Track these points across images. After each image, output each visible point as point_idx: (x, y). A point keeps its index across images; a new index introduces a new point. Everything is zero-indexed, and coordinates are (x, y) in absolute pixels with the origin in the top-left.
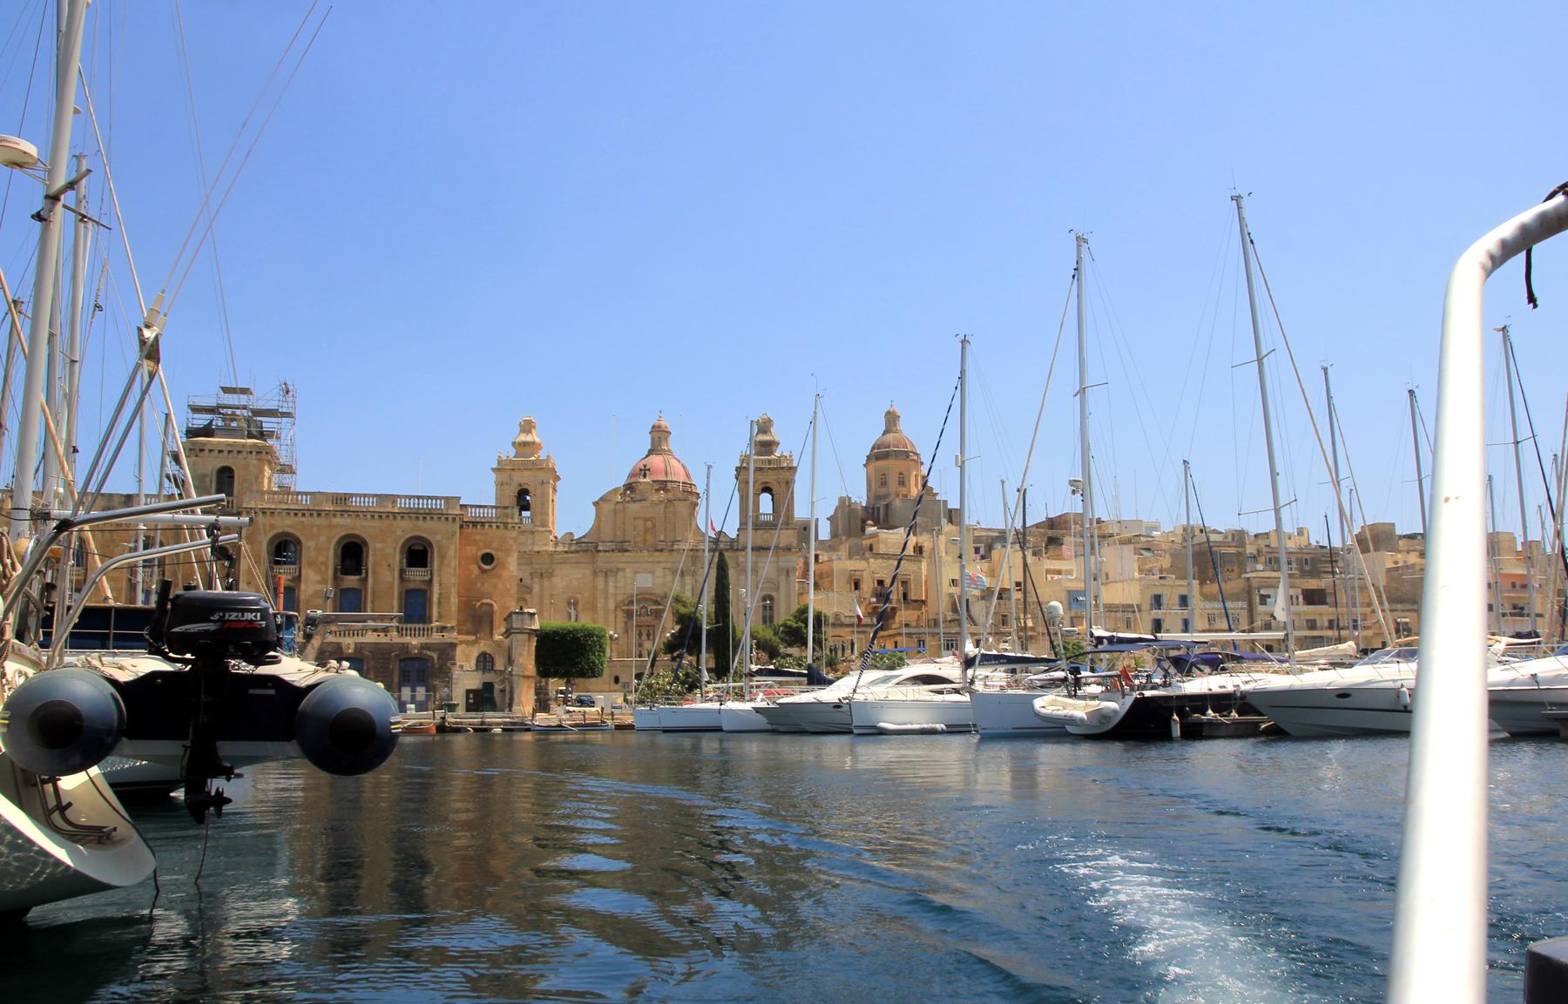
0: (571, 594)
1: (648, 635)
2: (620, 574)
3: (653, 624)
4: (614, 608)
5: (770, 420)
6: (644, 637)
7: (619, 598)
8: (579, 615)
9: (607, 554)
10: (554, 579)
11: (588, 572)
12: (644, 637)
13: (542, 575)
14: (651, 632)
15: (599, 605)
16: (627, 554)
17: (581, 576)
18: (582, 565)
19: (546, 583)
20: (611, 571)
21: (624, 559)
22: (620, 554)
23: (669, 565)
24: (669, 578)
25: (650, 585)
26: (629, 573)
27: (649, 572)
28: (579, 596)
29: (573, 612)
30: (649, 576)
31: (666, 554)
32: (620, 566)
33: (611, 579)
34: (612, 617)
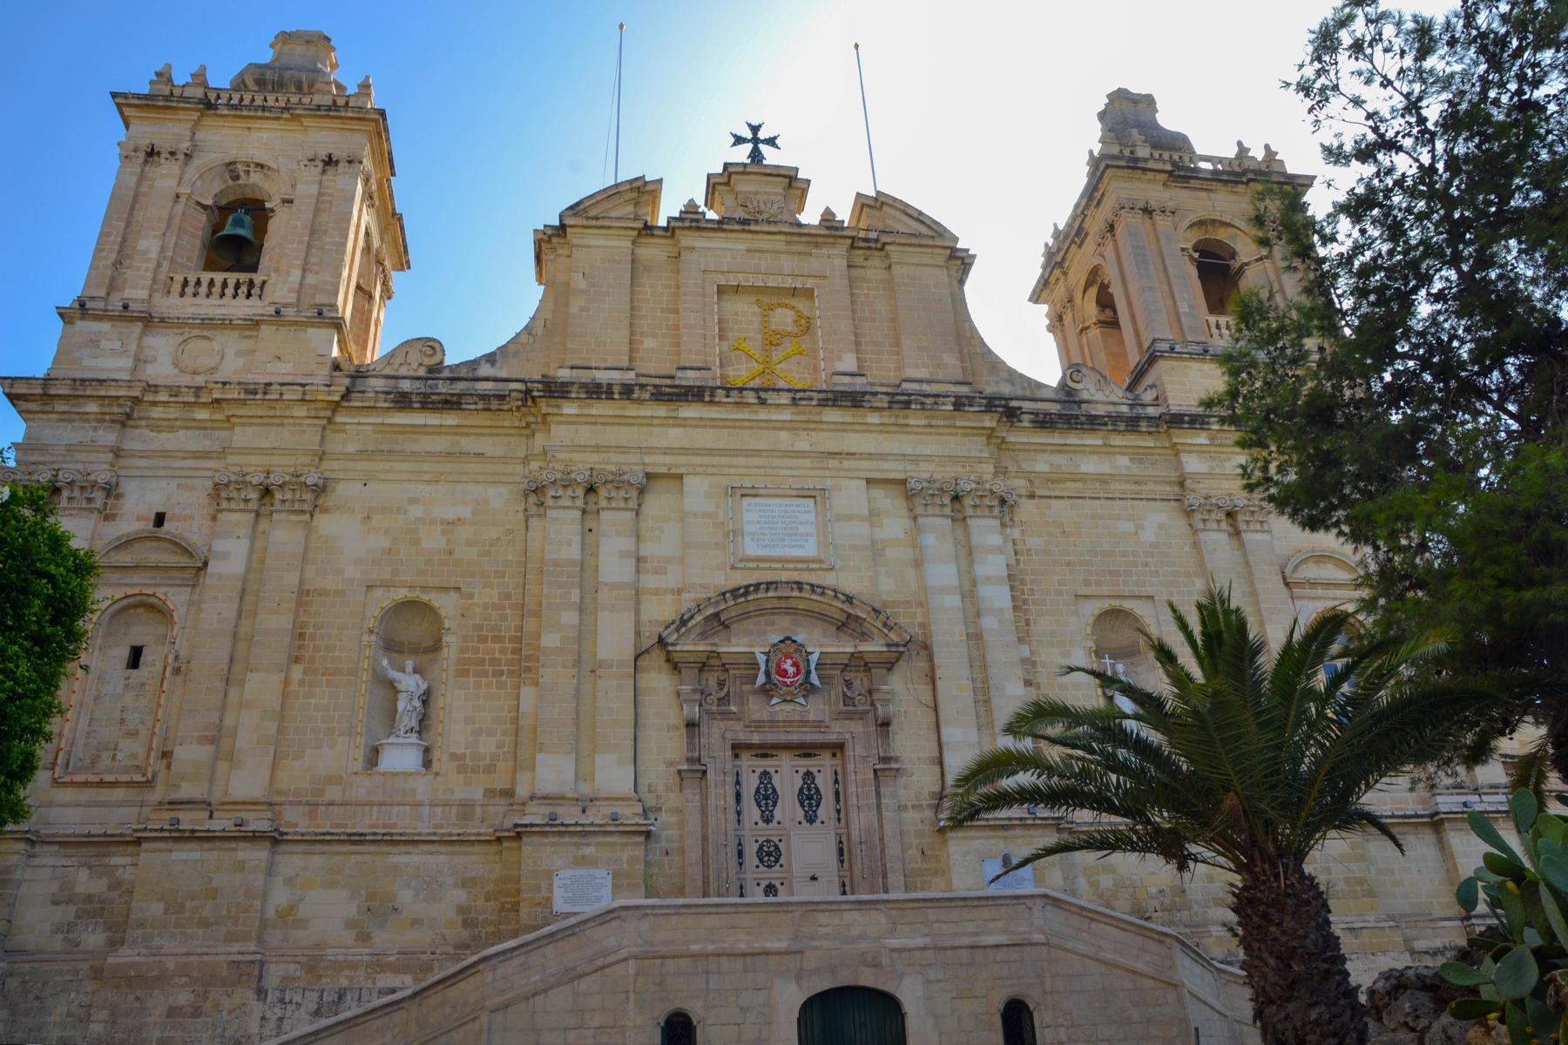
0: (401, 594)
1: (809, 798)
2: (657, 503)
3: (832, 738)
4: (629, 655)
5: (1120, 98)
6: (788, 808)
7: (660, 611)
8: (439, 701)
9: (600, 408)
10: (326, 524)
11: (501, 498)
12: (788, 808)
13: (267, 492)
14: (824, 783)
15: (550, 640)
16: (690, 411)
17: (465, 512)
18: (475, 467)
19: (284, 534)
20: (618, 481)
21: (675, 436)
22: (661, 411)
23: (894, 470)
24: (895, 526)
25: (809, 549)
26: (697, 490)
27: (803, 495)
28: (445, 604)
29: (410, 683)
30: (805, 510)
31: (874, 418)
32: (658, 463)
33: (613, 521)
34: (613, 698)
